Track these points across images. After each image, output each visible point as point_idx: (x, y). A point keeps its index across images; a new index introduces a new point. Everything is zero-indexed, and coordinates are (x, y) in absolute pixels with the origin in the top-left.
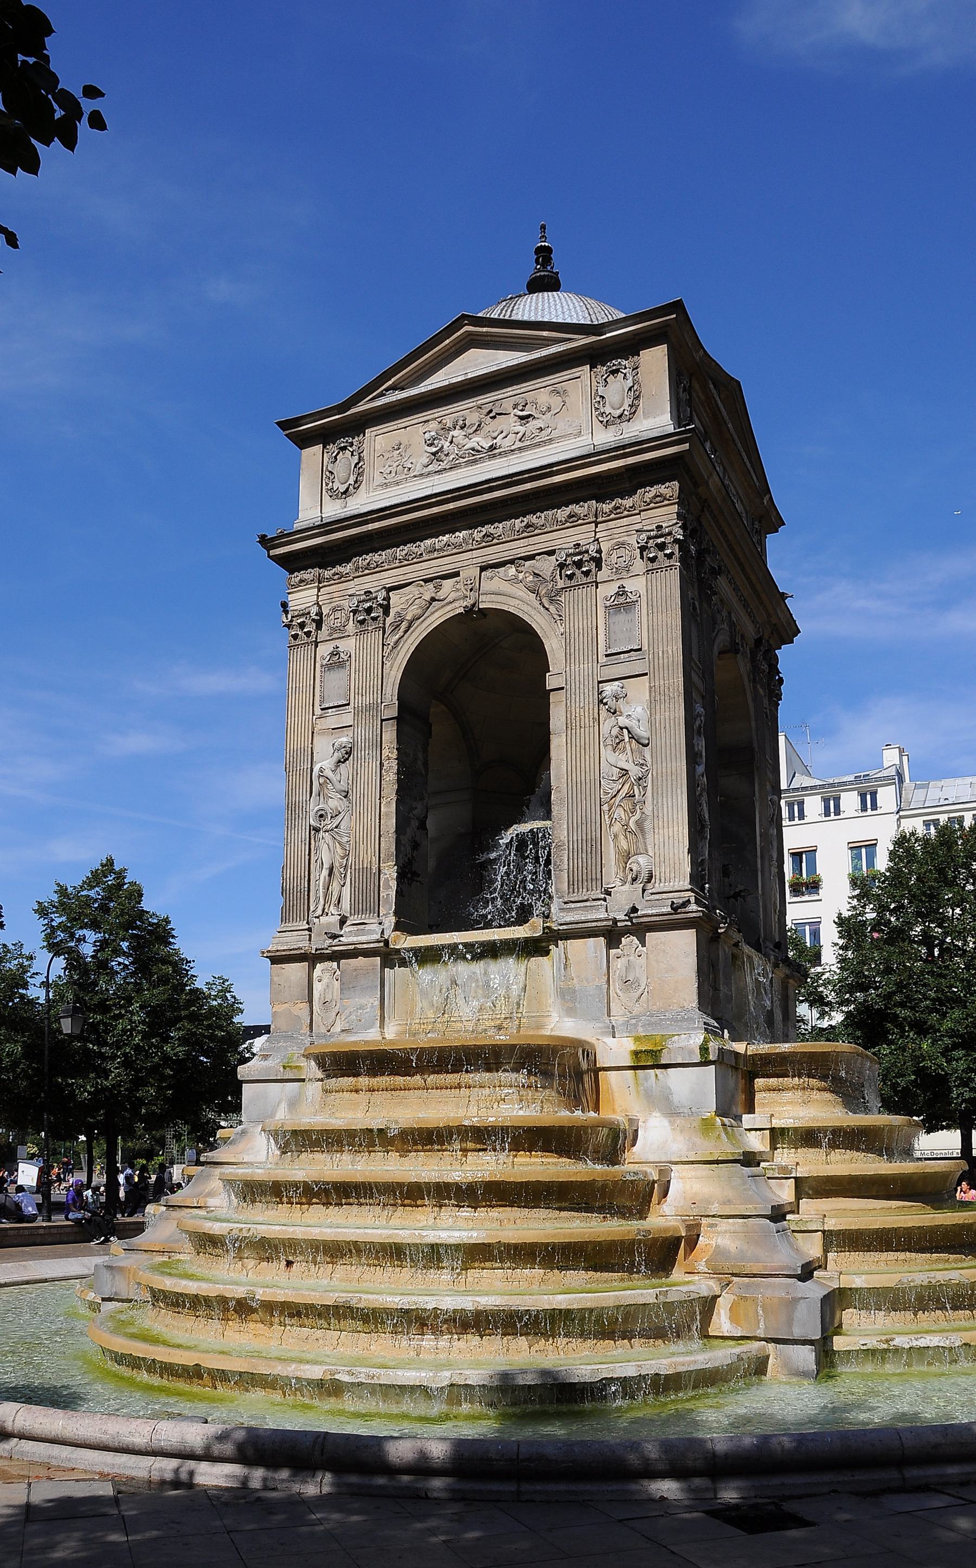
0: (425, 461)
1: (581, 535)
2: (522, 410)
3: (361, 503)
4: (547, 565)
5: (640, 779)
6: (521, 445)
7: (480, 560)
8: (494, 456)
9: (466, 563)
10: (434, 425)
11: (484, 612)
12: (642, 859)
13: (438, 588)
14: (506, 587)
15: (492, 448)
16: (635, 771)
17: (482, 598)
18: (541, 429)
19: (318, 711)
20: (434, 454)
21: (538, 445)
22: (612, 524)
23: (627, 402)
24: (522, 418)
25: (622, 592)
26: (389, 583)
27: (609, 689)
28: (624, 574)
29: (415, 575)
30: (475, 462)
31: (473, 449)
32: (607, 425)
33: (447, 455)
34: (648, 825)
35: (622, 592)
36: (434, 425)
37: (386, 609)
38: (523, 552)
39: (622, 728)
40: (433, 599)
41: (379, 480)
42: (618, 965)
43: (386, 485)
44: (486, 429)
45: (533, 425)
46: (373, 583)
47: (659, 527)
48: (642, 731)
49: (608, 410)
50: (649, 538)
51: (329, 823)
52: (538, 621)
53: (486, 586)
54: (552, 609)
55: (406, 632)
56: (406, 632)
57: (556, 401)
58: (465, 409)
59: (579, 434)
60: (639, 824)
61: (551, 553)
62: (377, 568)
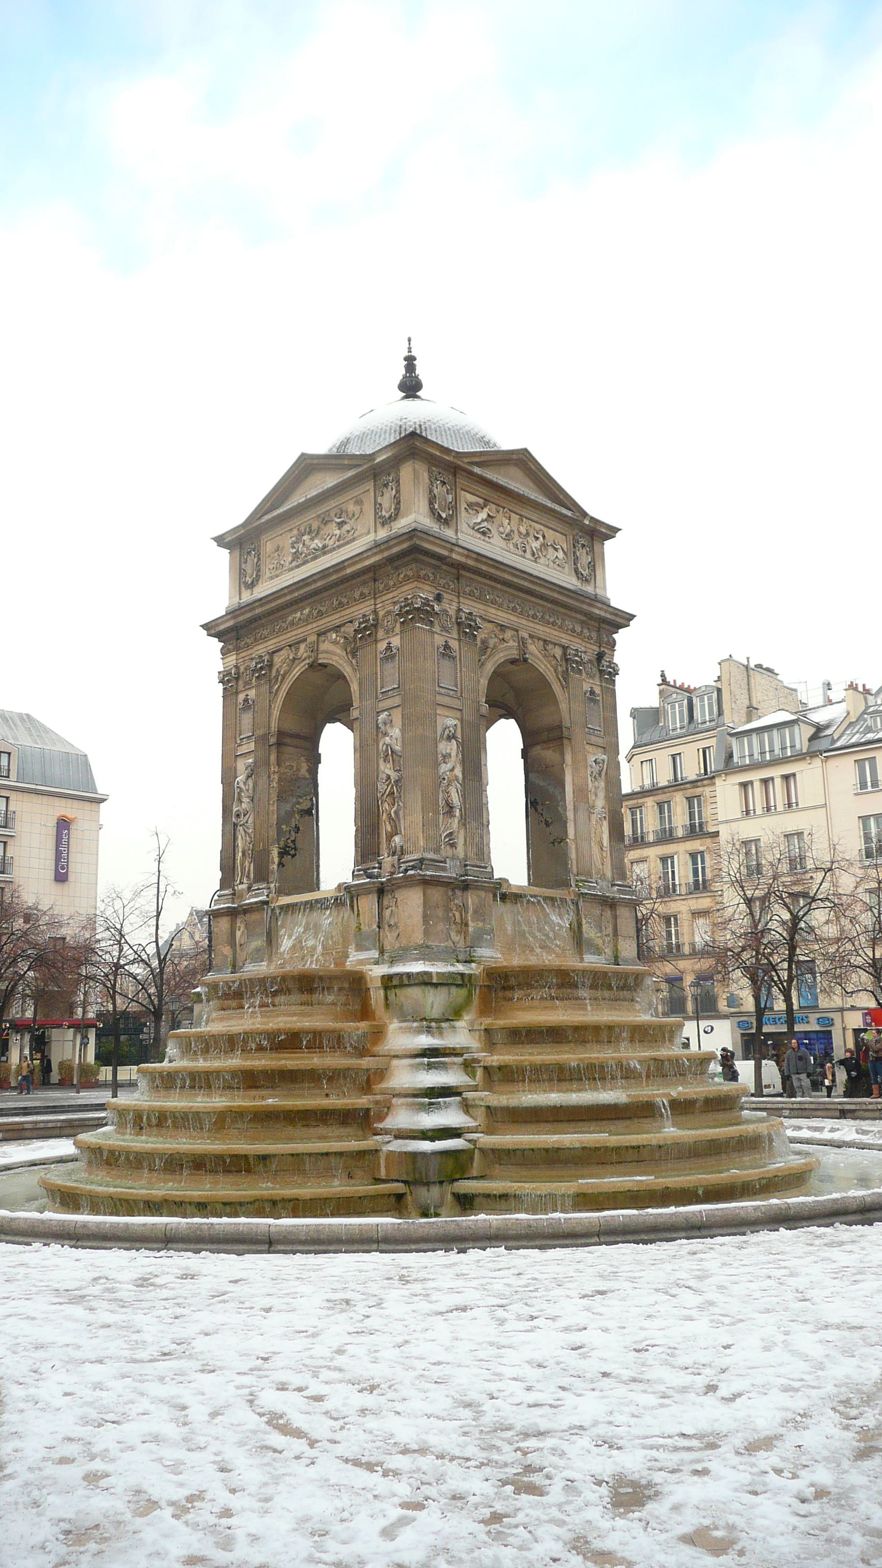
0: (290, 559)
1: (364, 608)
2: (340, 518)
3: (264, 589)
4: (350, 629)
5: (397, 781)
6: (337, 543)
7: (316, 629)
8: (325, 553)
9: (310, 632)
10: (295, 532)
11: (324, 666)
12: (397, 839)
13: (298, 649)
14: (332, 647)
15: (324, 547)
16: (394, 776)
17: (320, 656)
18: (348, 531)
19: (239, 742)
20: (295, 553)
21: (348, 543)
22: (384, 598)
23: (393, 507)
24: (339, 524)
25: (389, 648)
26: (271, 648)
27: (383, 716)
28: (391, 634)
29: (284, 642)
30: (315, 558)
31: (314, 549)
32: (383, 524)
33: (301, 554)
34: (401, 813)
35: (389, 648)
36: (295, 532)
37: (270, 665)
38: (338, 622)
39: (387, 745)
40: (294, 659)
41: (268, 575)
42: (387, 913)
43: (271, 578)
44: (322, 532)
45: (347, 527)
46: (261, 649)
47: (406, 599)
48: (398, 748)
49: (384, 513)
50: (401, 607)
51: (243, 820)
52: (347, 671)
53: (324, 646)
54: (354, 661)
55: (281, 682)
56: (281, 682)
57: (357, 509)
58: (310, 518)
59: (369, 533)
60: (396, 813)
61: (351, 622)
62: (265, 639)
